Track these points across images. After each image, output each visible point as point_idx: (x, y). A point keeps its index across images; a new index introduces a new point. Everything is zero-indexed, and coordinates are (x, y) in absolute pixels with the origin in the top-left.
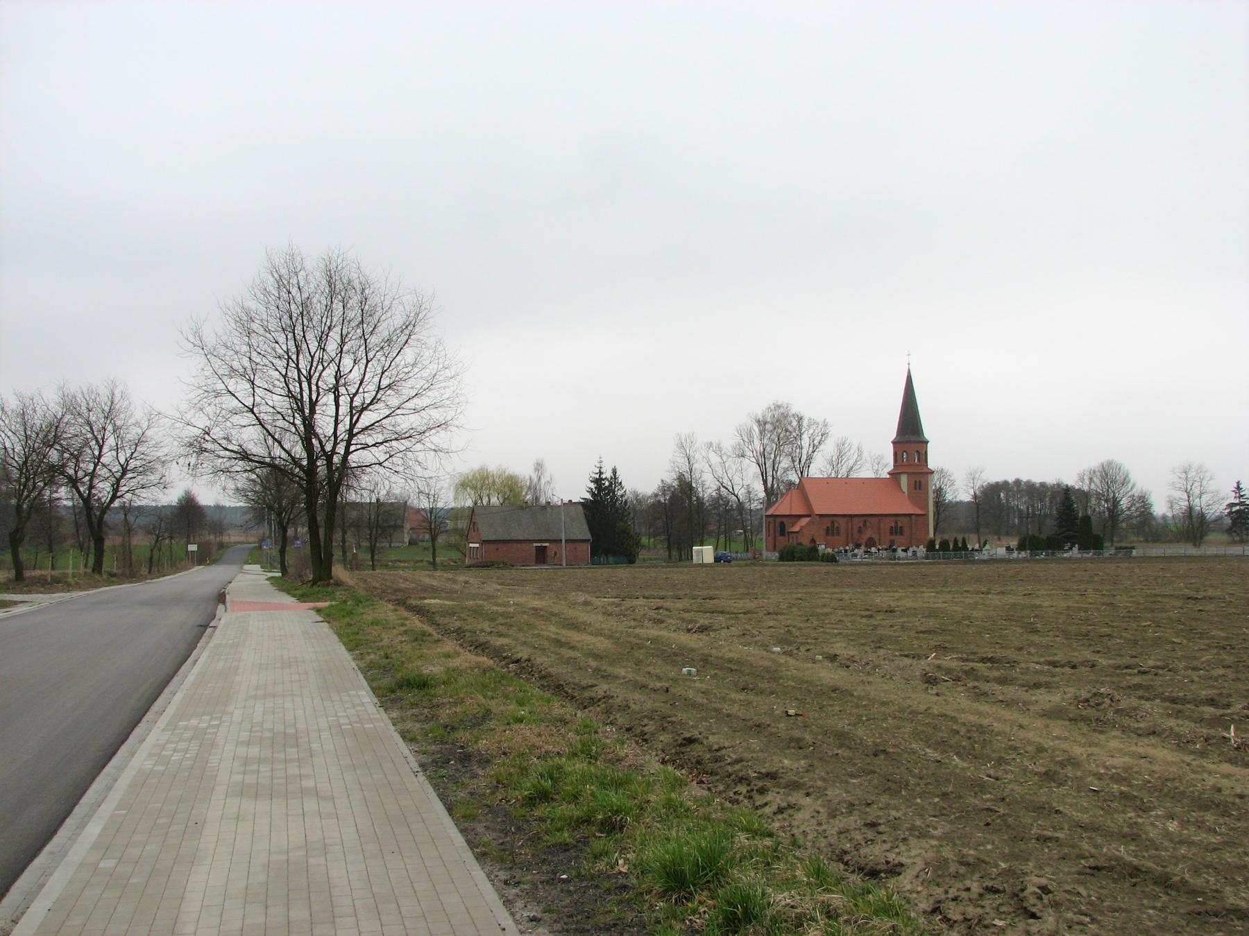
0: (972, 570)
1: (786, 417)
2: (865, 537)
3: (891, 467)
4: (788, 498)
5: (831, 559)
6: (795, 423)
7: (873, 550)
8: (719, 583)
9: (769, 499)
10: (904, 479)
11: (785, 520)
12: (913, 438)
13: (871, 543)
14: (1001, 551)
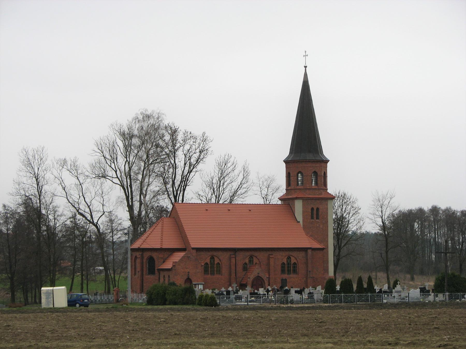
0: (378, 316)
1: (156, 130)
2: (252, 276)
3: (282, 191)
4: (159, 227)
5: (210, 303)
6: (167, 138)
7: (261, 291)
8: (72, 332)
9: (135, 230)
10: (298, 206)
11: (155, 255)
12: (310, 156)
13: (258, 282)
14: (415, 294)
